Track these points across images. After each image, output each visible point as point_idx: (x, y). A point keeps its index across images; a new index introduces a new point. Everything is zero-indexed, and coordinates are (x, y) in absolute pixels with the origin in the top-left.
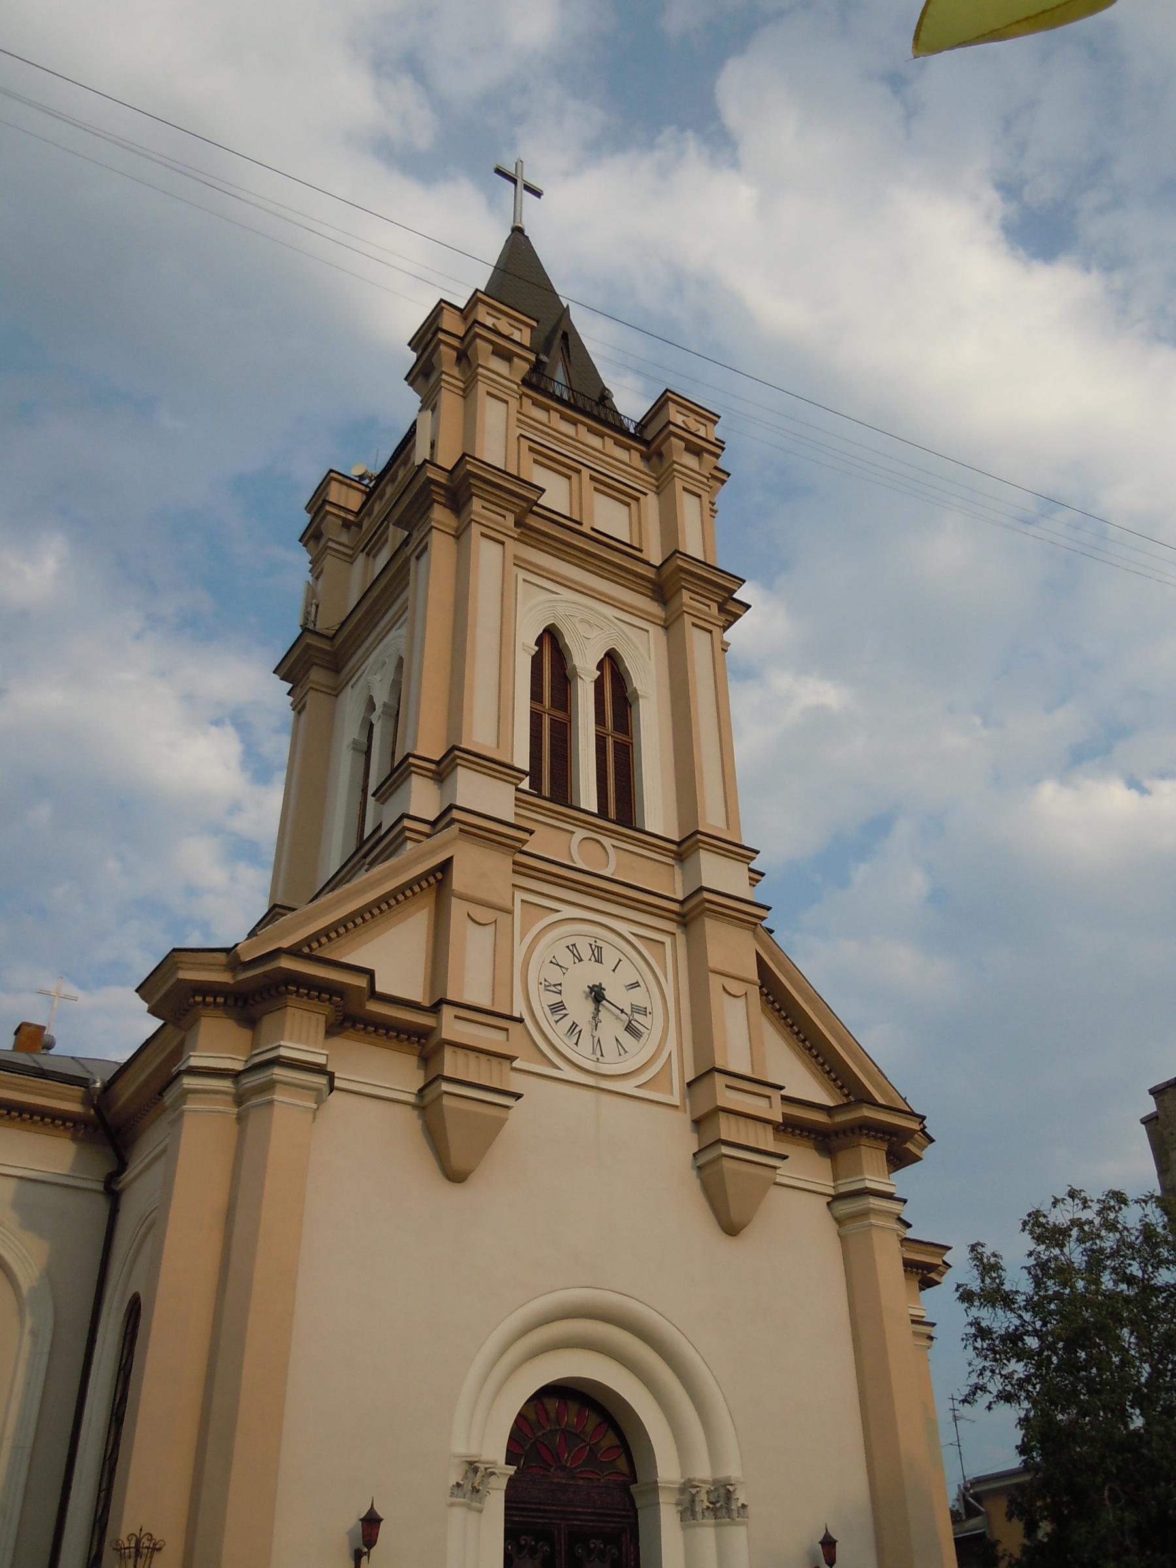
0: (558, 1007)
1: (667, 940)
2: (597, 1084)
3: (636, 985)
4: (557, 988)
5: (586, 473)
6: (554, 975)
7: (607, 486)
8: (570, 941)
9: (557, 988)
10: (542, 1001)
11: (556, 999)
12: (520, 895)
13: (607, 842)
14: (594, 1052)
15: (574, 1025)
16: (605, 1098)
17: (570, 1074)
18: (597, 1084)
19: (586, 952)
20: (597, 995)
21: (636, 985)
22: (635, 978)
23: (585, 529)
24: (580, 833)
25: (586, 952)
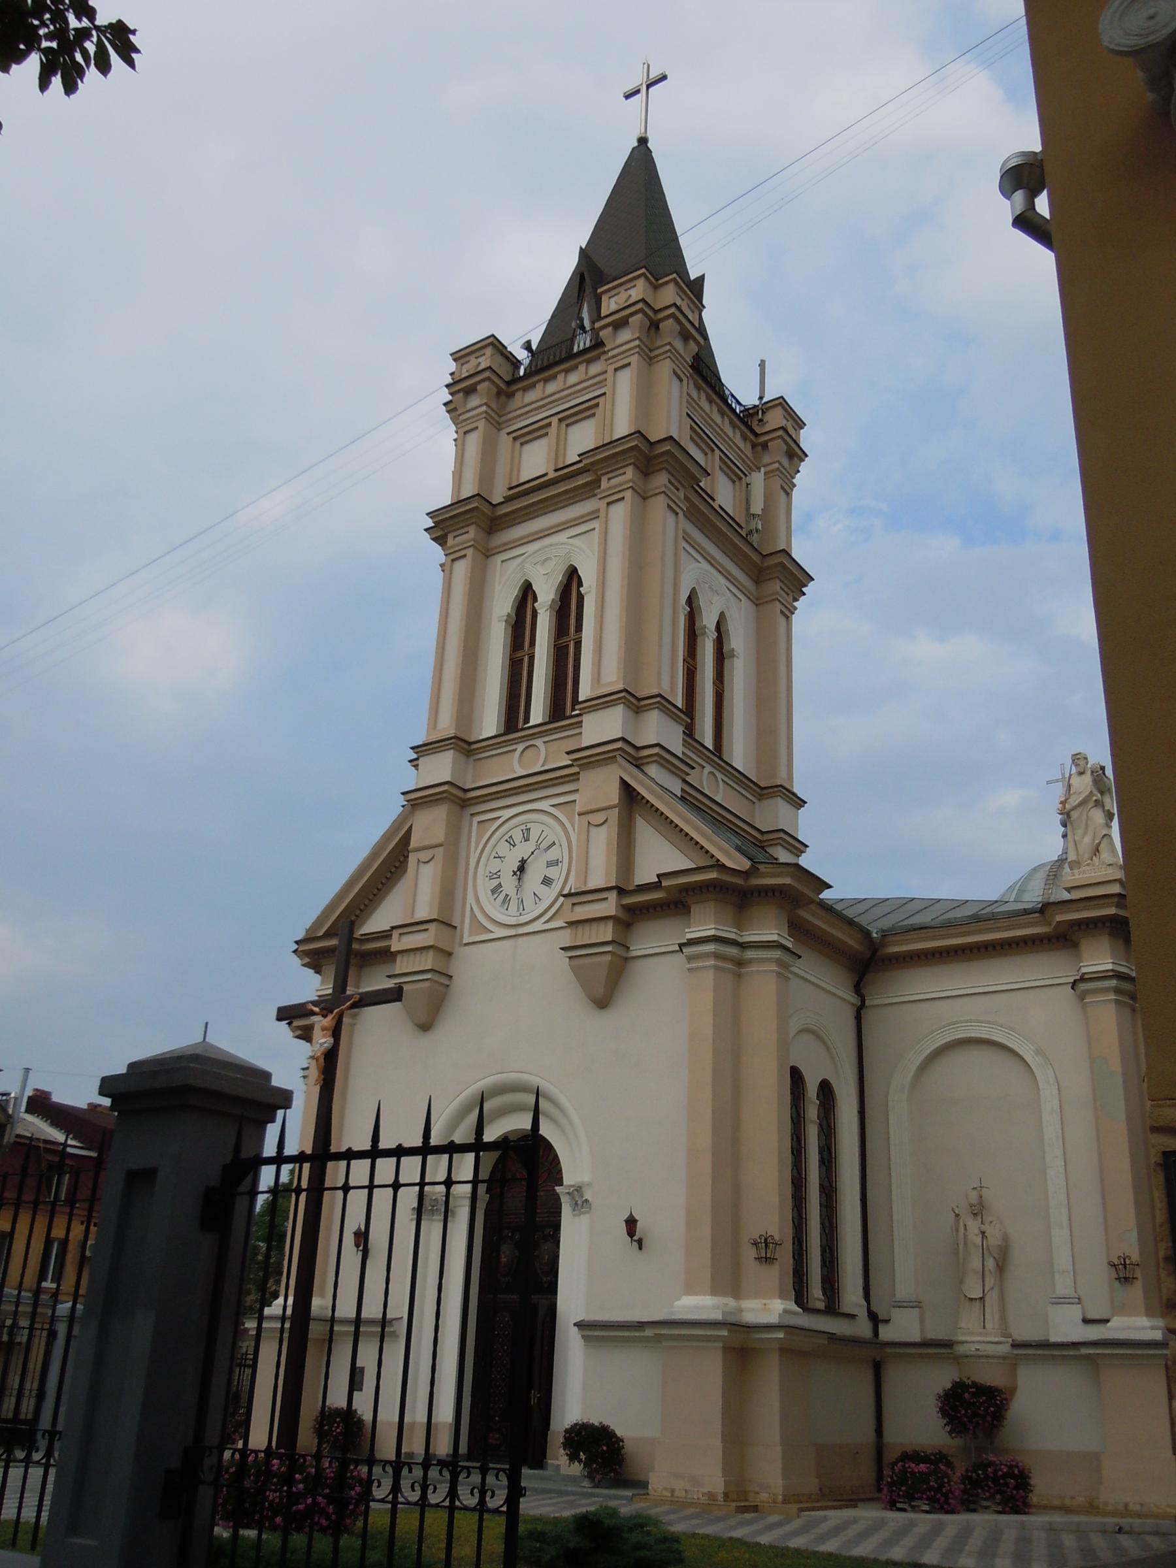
0: (496, 890)
3: (554, 843)
4: (497, 875)
6: (495, 865)
7: (570, 418)
9: (497, 875)
10: (484, 886)
11: (496, 882)
13: (539, 742)
16: (521, 939)
17: (500, 932)
18: (517, 932)
20: (522, 868)
21: (554, 843)
23: (552, 475)
25: (517, 835)
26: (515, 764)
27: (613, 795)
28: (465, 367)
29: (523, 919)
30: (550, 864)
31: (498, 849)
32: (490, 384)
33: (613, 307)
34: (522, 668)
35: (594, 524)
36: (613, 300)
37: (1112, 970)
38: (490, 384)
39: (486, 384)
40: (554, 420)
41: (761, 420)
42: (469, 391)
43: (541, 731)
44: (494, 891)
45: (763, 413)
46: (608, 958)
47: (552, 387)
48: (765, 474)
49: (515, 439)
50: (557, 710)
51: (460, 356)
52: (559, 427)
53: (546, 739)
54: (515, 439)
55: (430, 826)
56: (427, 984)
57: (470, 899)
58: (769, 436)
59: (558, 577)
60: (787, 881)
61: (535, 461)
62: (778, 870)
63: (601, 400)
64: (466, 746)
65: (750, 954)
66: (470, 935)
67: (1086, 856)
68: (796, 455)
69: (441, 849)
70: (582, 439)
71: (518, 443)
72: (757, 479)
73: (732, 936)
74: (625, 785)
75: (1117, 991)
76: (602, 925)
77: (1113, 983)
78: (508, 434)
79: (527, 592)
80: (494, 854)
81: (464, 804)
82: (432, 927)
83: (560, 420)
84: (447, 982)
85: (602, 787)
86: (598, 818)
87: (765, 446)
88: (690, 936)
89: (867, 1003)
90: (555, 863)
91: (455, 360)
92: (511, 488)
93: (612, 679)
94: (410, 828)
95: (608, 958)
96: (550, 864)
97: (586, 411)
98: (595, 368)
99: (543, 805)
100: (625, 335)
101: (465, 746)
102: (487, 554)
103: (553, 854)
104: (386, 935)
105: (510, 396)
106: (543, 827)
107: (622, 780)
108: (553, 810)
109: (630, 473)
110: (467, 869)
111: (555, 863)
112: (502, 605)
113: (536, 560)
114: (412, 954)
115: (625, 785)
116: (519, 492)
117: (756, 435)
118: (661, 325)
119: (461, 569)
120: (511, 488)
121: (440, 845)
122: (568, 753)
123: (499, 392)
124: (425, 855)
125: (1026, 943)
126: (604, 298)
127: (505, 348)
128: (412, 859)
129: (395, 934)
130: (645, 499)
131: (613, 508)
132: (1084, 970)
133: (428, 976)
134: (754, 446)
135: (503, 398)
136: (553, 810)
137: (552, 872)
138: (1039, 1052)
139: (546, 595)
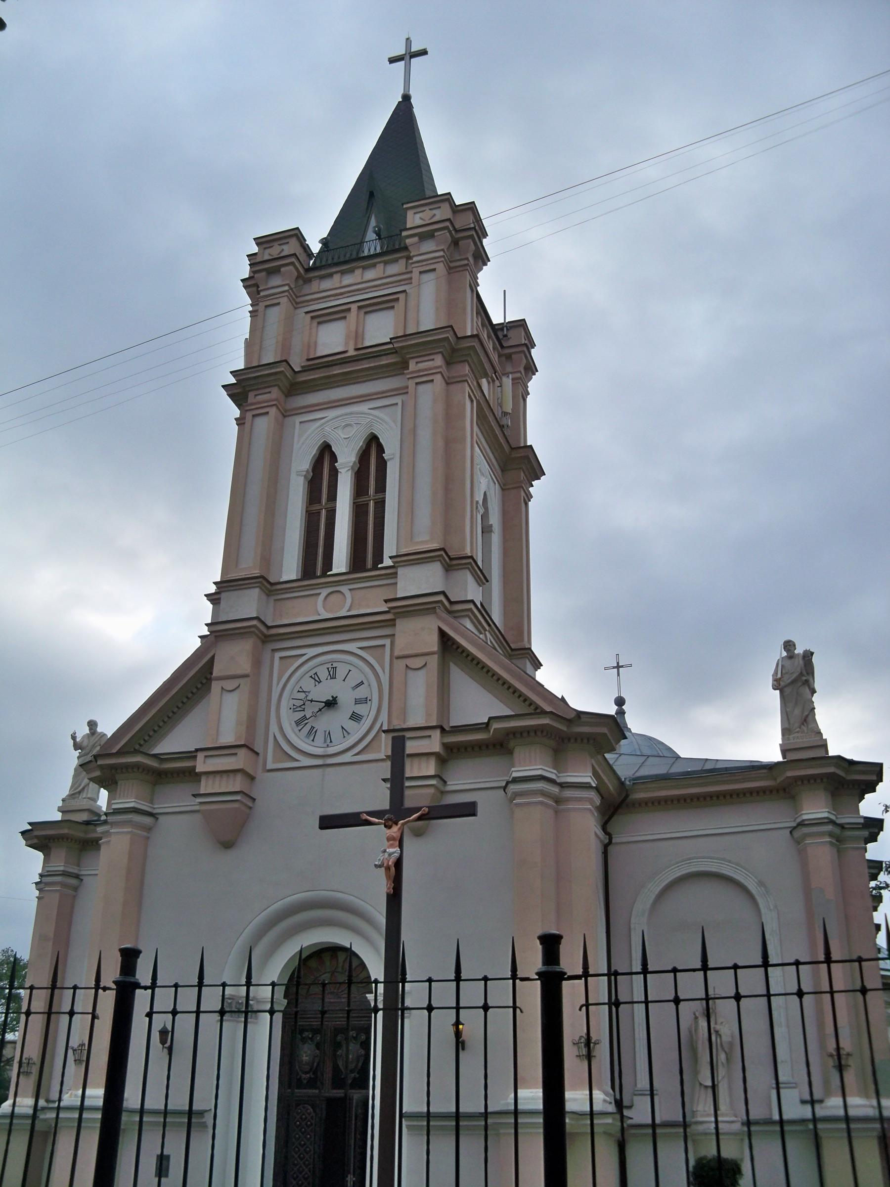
1: (387, 642)
2: (324, 762)
3: (362, 683)
5: (354, 307)
7: (371, 307)
8: (311, 673)
10: (288, 719)
12: (278, 655)
13: (344, 589)
14: (325, 742)
15: (313, 727)
18: (324, 762)
19: (323, 673)
21: (362, 683)
22: (360, 678)
23: (352, 353)
24: (325, 592)
25: (323, 673)
26: (319, 606)
27: (432, 643)
28: (267, 251)
29: (331, 750)
30: (358, 702)
31: (302, 683)
32: (278, 267)
33: (418, 222)
34: (319, 520)
35: (398, 400)
36: (418, 216)
37: (827, 818)
38: (278, 267)
39: (291, 267)
40: (354, 307)
41: (505, 336)
42: (273, 272)
43: (341, 580)
44: (298, 723)
45: (507, 330)
46: (432, 791)
47: (348, 280)
48: (513, 379)
49: (312, 318)
50: (357, 562)
51: (259, 241)
52: (358, 315)
53: (351, 587)
54: (312, 318)
55: (235, 657)
56: (236, 805)
57: (274, 728)
58: (509, 349)
59: (359, 443)
60: (604, 730)
61: (332, 339)
62: (593, 720)
63: (402, 296)
64: (268, 586)
65: (568, 793)
66: (274, 762)
67: (797, 725)
68: (531, 369)
69: (248, 679)
70: (380, 329)
71: (315, 322)
72: (507, 382)
73: (554, 777)
74: (442, 634)
75: (831, 834)
76: (424, 759)
77: (830, 827)
78: (306, 313)
79: (326, 453)
80: (297, 688)
81: (266, 639)
82: (242, 752)
83: (360, 308)
84: (250, 804)
85: (421, 635)
86: (417, 662)
87: (509, 357)
88: (515, 775)
89: (614, 841)
90: (365, 701)
91: (257, 244)
92: (308, 360)
93: (426, 538)
94: (213, 658)
95: (432, 791)
96: (358, 702)
97: (385, 303)
98: (393, 269)
99: (352, 647)
100: (429, 246)
101: (269, 587)
102: (286, 414)
103: (362, 692)
104: (192, 755)
105: (308, 281)
106: (349, 667)
107: (440, 630)
108: (360, 652)
109: (439, 361)
110: (269, 700)
111: (365, 701)
112: (301, 462)
113: (341, 426)
114: (225, 776)
115: (442, 634)
116: (317, 364)
117: (502, 347)
118: (460, 243)
119: (263, 426)
120: (308, 360)
121: (246, 676)
122: (386, 601)
123: (299, 277)
124: (230, 685)
125: (764, 792)
126: (410, 214)
127: (305, 240)
128: (216, 686)
129: (201, 756)
130: (447, 384)
131: (421, 388)
132: (805, 817)
133: (238, 797)
134: (500, 356)
135: (301, 282)
136: (360, 652)
137: (361, 709)
138: (761, 884)
139: (346, 459)
